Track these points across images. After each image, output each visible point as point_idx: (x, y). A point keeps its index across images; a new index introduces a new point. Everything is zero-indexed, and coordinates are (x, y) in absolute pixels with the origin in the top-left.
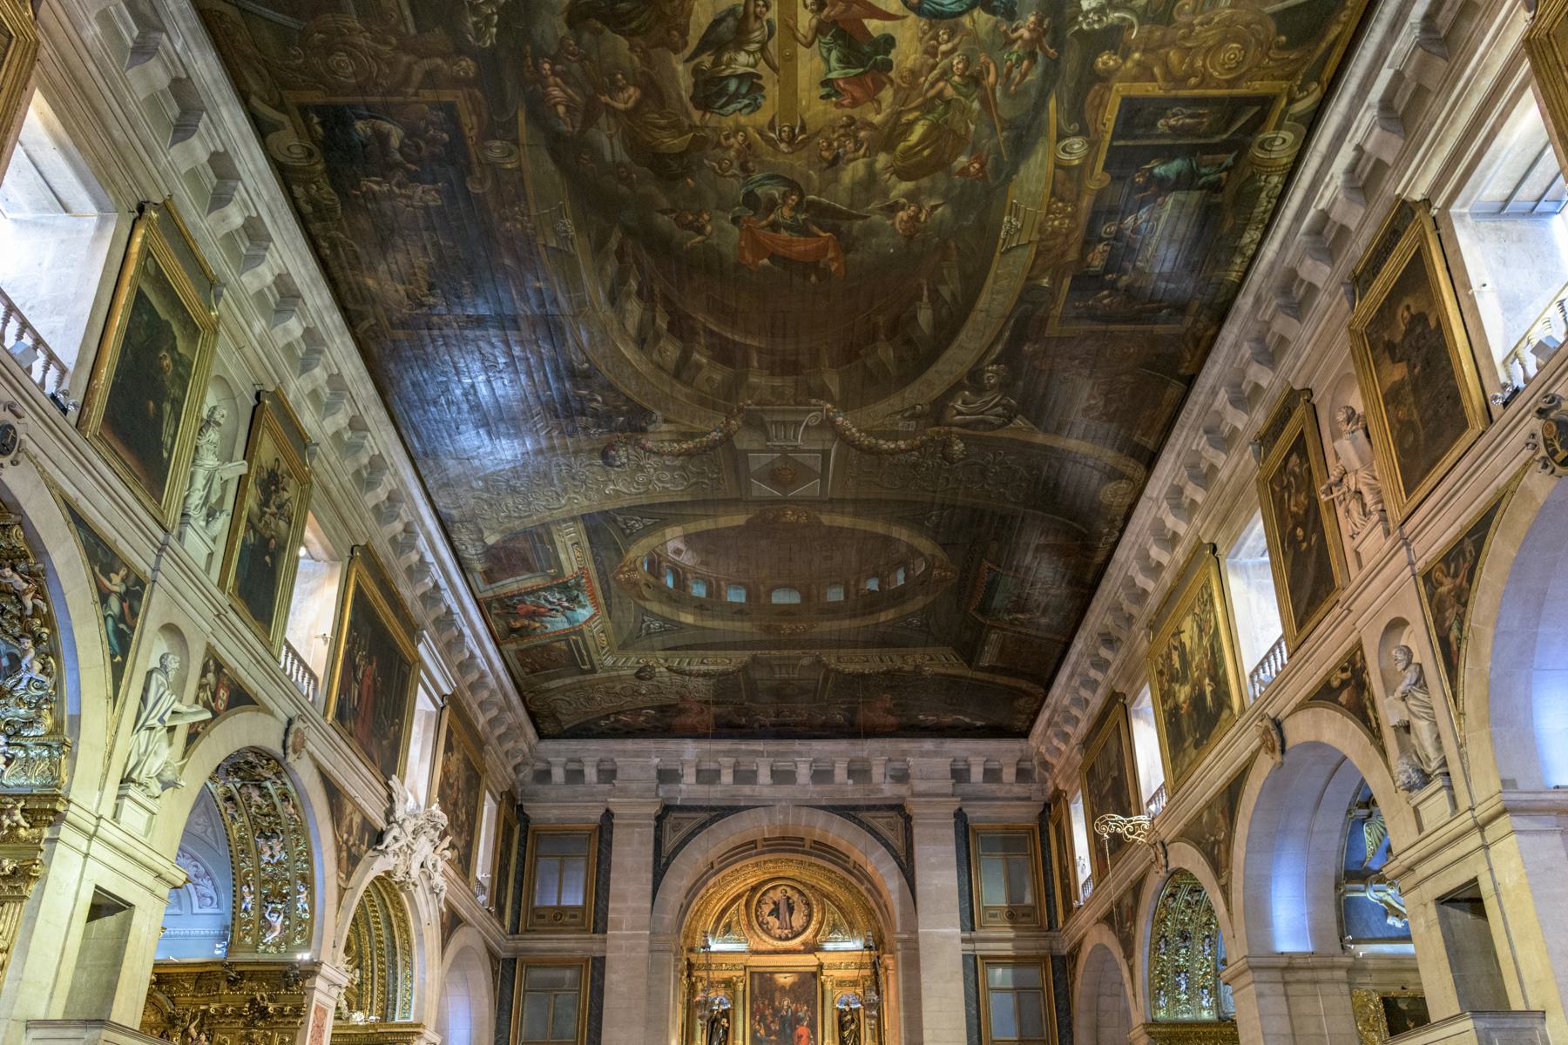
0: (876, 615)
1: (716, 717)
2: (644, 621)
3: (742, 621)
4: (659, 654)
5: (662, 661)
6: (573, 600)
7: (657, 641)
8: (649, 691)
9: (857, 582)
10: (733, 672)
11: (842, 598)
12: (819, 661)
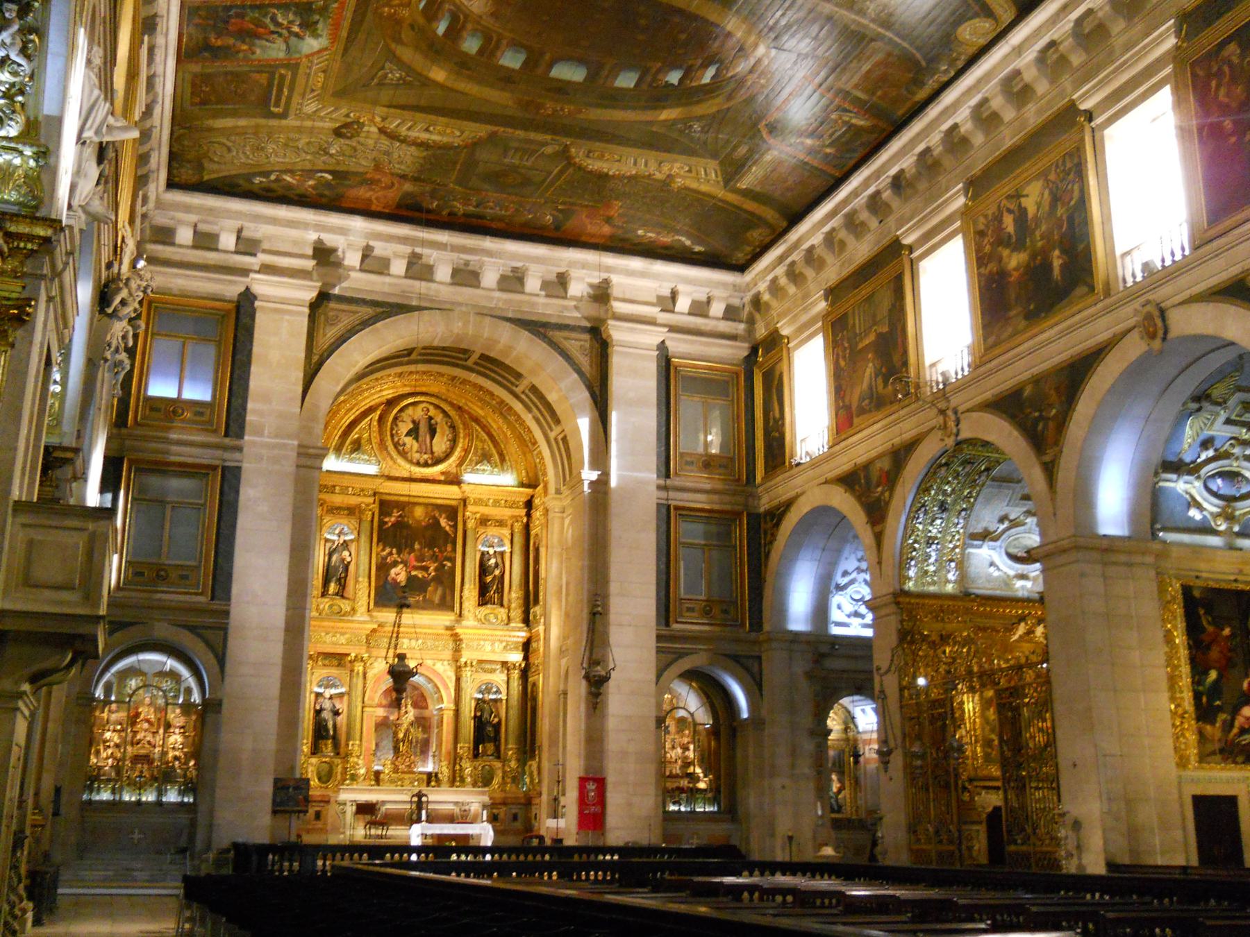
0: (658, 112)
1: (407, 195)
2: (383, 68)
3: (503, 89)
4: (380, 110)
5: (378, 119)
6: (309, 27)
7: (386, 95)
8: (341, 153)
9: (659, 71)
10: (459, 146)
11: (632, 86)
12: (564, 154)
